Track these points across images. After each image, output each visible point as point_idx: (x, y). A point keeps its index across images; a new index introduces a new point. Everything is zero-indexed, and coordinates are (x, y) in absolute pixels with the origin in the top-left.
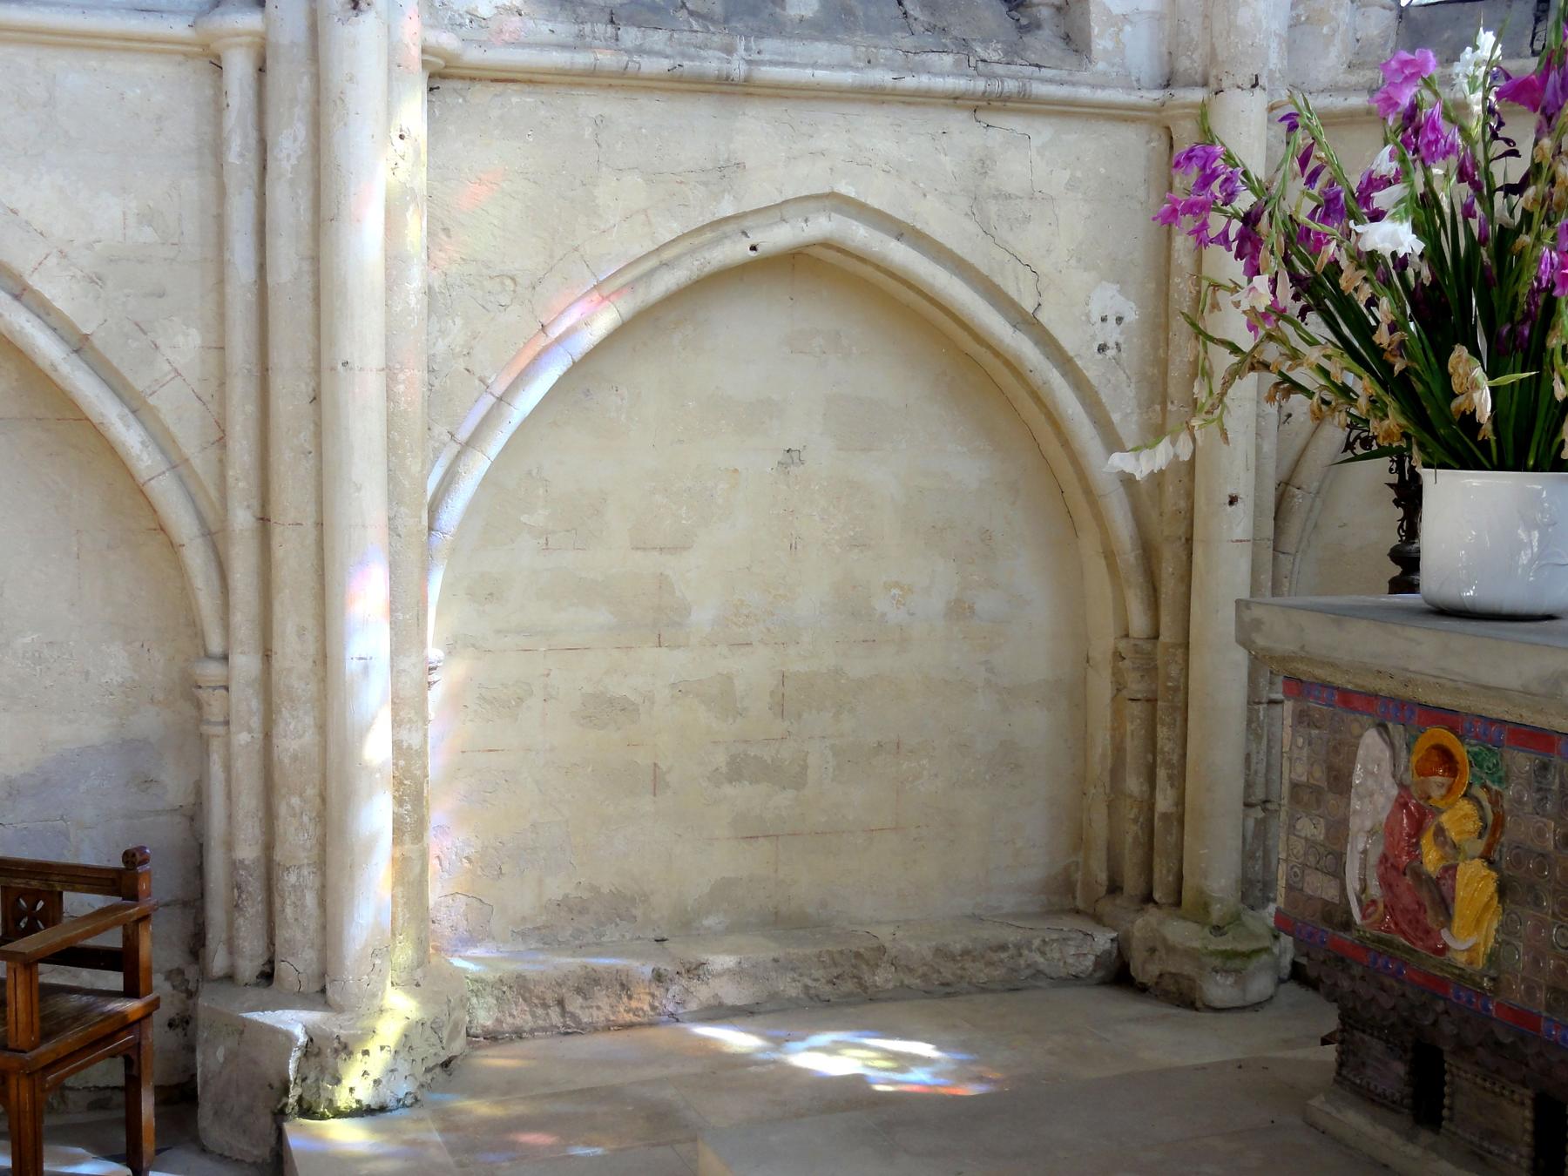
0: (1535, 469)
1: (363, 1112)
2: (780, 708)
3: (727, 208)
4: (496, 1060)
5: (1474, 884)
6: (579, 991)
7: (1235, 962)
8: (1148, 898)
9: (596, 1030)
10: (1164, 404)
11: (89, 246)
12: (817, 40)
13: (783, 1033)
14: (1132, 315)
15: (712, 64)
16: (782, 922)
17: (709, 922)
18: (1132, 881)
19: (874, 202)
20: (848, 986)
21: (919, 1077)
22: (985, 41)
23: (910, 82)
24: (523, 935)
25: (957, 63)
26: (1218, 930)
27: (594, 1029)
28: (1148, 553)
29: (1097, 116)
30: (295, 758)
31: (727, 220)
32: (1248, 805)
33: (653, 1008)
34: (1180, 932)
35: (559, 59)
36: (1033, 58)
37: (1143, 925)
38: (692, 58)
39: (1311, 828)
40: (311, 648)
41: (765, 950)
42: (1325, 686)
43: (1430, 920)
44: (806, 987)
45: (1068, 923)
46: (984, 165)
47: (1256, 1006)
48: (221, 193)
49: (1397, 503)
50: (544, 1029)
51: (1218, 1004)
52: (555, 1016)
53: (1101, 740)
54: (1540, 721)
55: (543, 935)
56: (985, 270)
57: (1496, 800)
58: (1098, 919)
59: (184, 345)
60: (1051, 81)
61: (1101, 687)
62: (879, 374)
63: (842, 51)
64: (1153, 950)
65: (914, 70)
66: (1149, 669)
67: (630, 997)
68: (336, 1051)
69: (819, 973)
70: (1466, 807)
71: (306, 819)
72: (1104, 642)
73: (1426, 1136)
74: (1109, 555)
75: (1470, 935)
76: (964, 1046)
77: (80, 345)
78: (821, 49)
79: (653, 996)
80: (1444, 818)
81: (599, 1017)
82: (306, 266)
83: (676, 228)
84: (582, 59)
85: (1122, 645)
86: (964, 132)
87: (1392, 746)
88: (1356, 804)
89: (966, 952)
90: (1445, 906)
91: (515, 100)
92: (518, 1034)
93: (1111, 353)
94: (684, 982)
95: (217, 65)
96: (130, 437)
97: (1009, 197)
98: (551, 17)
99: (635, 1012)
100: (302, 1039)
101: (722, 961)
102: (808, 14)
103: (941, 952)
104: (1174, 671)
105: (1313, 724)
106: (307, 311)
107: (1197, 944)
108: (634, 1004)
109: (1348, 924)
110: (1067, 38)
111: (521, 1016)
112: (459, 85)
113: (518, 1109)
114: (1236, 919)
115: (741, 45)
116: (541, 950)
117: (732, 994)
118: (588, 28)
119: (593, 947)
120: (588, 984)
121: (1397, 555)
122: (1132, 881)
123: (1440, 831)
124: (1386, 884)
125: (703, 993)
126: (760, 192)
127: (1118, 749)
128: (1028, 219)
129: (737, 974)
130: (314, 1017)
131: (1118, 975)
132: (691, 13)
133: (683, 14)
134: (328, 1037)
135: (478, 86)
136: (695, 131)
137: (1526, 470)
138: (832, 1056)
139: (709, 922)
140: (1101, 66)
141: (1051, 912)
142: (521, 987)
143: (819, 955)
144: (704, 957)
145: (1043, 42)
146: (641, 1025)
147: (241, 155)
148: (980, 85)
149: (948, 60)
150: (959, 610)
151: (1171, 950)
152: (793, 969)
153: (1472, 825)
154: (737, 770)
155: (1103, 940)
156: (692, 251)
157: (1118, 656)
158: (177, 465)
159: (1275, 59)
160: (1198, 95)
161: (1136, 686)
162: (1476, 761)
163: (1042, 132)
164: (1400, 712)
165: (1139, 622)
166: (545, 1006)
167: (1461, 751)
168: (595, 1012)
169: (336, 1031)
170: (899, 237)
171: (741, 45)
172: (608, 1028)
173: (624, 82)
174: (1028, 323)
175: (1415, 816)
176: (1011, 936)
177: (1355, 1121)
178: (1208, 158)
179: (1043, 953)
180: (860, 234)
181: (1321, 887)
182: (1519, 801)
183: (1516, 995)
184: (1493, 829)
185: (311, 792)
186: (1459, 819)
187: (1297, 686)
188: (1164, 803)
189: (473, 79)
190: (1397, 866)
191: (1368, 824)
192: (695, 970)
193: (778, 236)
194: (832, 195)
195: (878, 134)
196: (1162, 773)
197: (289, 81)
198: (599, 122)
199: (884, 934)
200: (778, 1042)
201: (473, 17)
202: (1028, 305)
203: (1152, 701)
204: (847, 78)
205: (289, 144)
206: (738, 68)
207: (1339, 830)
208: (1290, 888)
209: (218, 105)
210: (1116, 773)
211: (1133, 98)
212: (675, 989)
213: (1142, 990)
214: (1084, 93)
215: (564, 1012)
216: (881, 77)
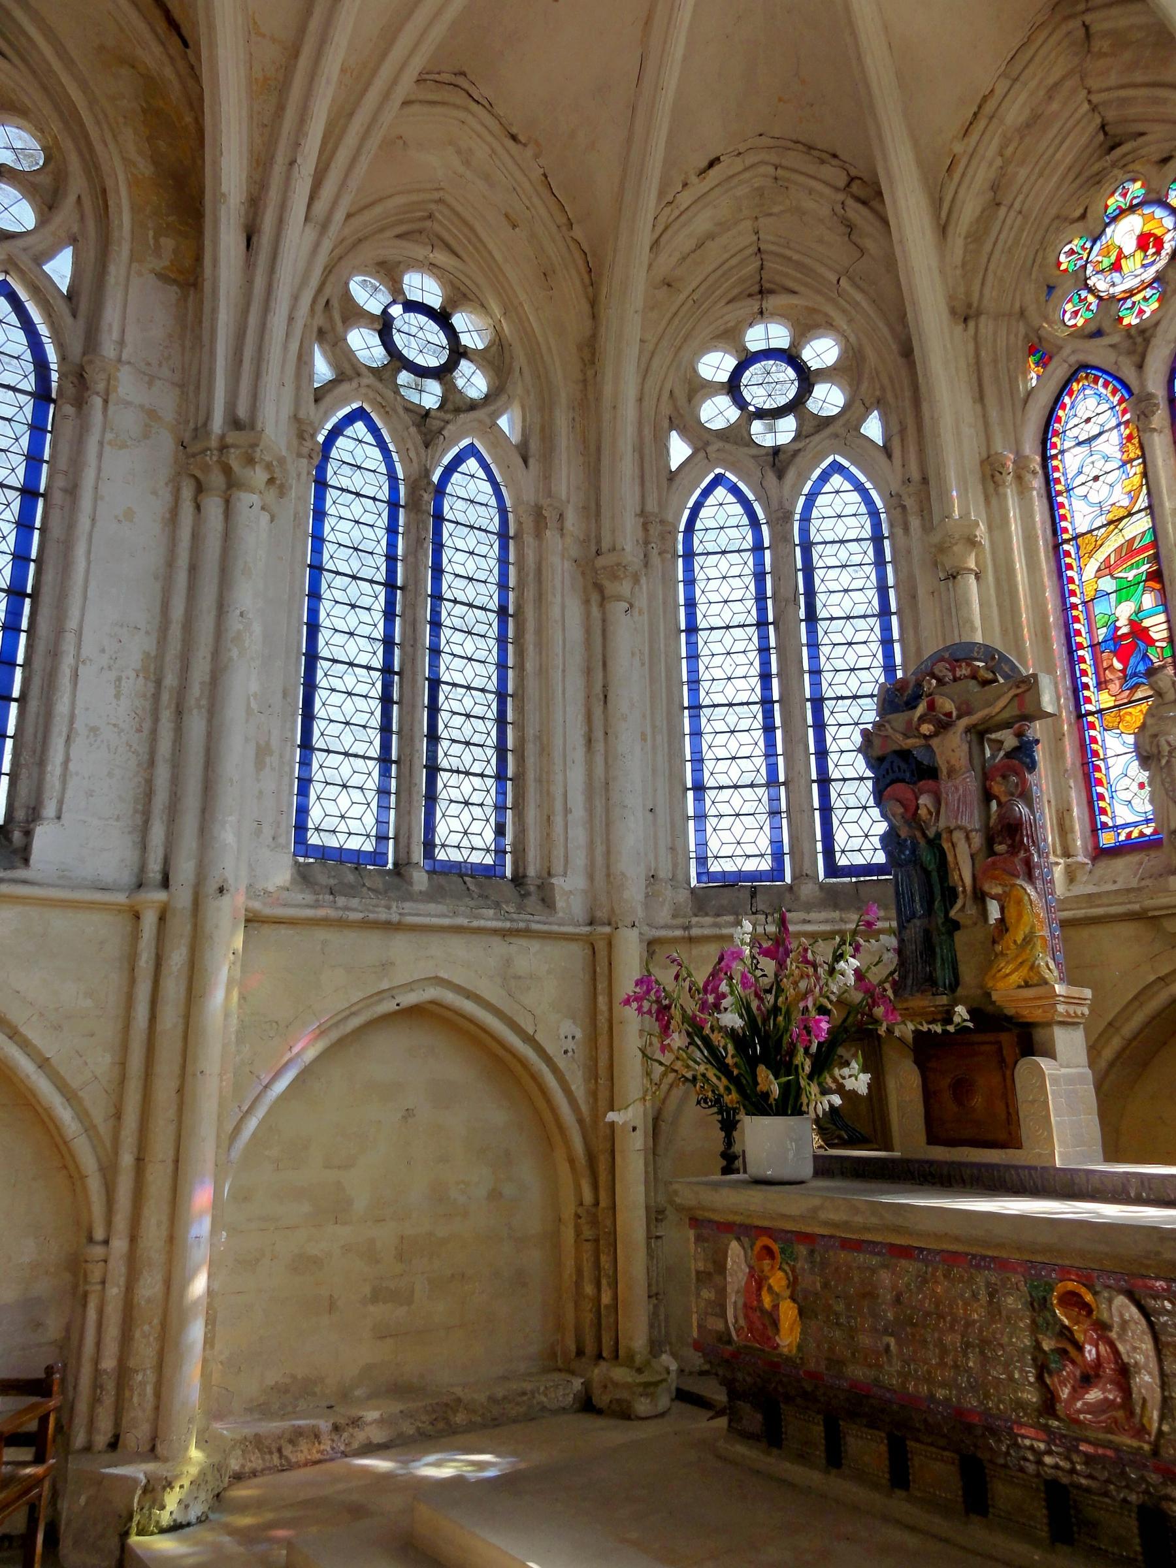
0: (792, 1115)
1: (176, 1527)
2: (400, 1257)
3: (385, 985)
4: (242, 1492)
5: (788, 1312)
6: (291, 1441)
7: (649, 1389)
8: (600, 1356)
9: (299, 1466)
10: (596, 1081)
11: (57, 1009)
12: (429, 902)
13: (410, 1458)
14: (579, 1035)
15: (383, 916)
16: (398, 1389)
17: (357, 1393)
18: (590, 1348)
19: (456, 981)
20: (441, 1425)
21: (491, 1473)
22: (507, 903)
23: (475, 923)
24: (249, 1410)
25: (495, 914)
26: (639, 1371)
27: (298, 1466)
29: (560, 938)
30: (149, 1301)
31: (384, 991)
32: (649, 1297)
33: (333, 1449)
34: (620, 1374)
35: (309, 913)
36: (529, 910)
37: (598, 1372)
38: (373, 912)
39: (707, 1294)
40: (164, 1233)
41: (396, 1407)
42: (710, 1221)
43: (770, 1333)
44: (418, 1428)
45: (556, 1376)
46: (508, 962)
47: (662, 1415)
48: (132, 981)
49: (722, 1129)
50: (270, 1469)
51: (643, 1415)
52: (276, 1460)
53: (569, 1264)
54: (809, 1230)
55: (263, 1410)
56: (509, 1014)
57: (793, 1270)
58: (573, 1373)
59: (102, 1062)
60: (539, 922)
61: (568, 1234)
62: (453, 1067)
63: (441, 908)
64: (605, 1387)
65: (477, 917)
66: (594, 1222)
67: (320, 1443)
68: (164, 1488)
69: (424, 1418)
70: (780, 1274)
71: (151, 1339)
72: (569, 1210)
73: (775, 1451)
74: (571, 1161)
75: (788, 1338)
76: (514, 1453)
77: (43, 1063)
78: (432, 907)
79: (333, 1441)
80: (771, 1281)
81: (301, 1457)
82: (181, 1021)
83: (361, 995)
84: (321, 913)
85: (580, 1211)
86: (499, 947)
87: (744, 1248)
88: (729, 1279)
89: (505, 1398)
90: (775, 1324)
91: (283, 932)
92: (254, 1474)
93: (570, 1054)
94: (351, 1430)
95: (137, 917)
96: (65, 1115)
97: (520, 977)
98: (302, 891)
99: (322, 1452)
100: (144, 1481)
101: (372, 1415)
102: (423, 889)
103: (492, 1399)
104: (609, 1223)
105: (705, 1240)
106: (179, 1044)
107: (630, 1380)
108: (322, 1447)
109: (730, 1341)
110: (543, 900)
111: (256, 1461)
112: (256, 925)
113: (269, 1516)
114: (648, 1363)
115: (394, 905)
116: (260, 1420)
117: (378, 1435)
118: (321, 897)
119: (291, 1417)
120: (295, 1437)
121: (724, 1155)
122: (590, 1348)
123: (770, 1288)
124: (746, 1316)
125: (361, 1436)
126: (401, 978)
127: (579, 1271)
128: (529, 988)
129: (381, 1422)
130: (150, 1467)
131: (587, 1405)
132: (369, 889)
133: (364, 890)
134: (160, 1479)
135: (266, 925)
136: (372, 946)
137: (786, 1115)
138: (437, 1468)
139: (357, 1393)
140: (561, 914)
141: (546, 1370)
142: (257, 1442)
143: (425, 1407)
144: (361, 1413)
145: (532, 901)
146: (326, 1461)
147: (147, 962)
148: (508, 925)
149: (491, 912)
150: (495, 1195)
151: (616, 1385)
152: (411, 1417)
153: (784, 1283)
154: (377, 1296)
155: (577, 1384)
156: (368, 1006)
157: (578, 1216)
158: (89, 1129)
159: (640, 913)
160: (607, 929)
161: (588, 1233)
162: (783, 1251)
163: (535, 946)
164: (745, 1231)
165: (588, 1197)
166: (271, 1453)
167: (775, 1247)
168: (299, 1455)
169: (165, 1474)
170: (468, 998)
171: (394, 905)
172: (306, 1465)
173: (341, 924)
174: (530, 1040)
175: (758, 1281)
176: (528, 1386)
177: (741, 1449)
178: (649, 983)
179: (546, 1395)
180: (450, 997)
181: (715, 1324)
182: (803, 1269)
183: (812, 1365)
184: (793, 1284)
185: (156, 1321)
186: (778, 1280)
187: (695, 1222)
188: (606, 1299)
189: (263, 922)
190: (752, 1307)
191: (736, 1288)
192: (356, 1422)
193: (410, 999)
194: (436, 977)
195: (458, 947)
196: (604, 1282)
197: (180, 927)
198: (325, 943)
199: (458, 1391)
200: (405, 1463)
201: (266, 892)
202: (531, 1032)
203: (597, 1241)
204: (446, 922)
205: (177, 958)
206: (395, 918)
207: (722, 1292)
208: (700, 1327)
209: (136, 935)
210: (578, 1285)
211: (577, 930)
212: (345, 1435)
213: (599, 1412)
214: (555, 928)
215: (281, 1456)
216: (462, 921)
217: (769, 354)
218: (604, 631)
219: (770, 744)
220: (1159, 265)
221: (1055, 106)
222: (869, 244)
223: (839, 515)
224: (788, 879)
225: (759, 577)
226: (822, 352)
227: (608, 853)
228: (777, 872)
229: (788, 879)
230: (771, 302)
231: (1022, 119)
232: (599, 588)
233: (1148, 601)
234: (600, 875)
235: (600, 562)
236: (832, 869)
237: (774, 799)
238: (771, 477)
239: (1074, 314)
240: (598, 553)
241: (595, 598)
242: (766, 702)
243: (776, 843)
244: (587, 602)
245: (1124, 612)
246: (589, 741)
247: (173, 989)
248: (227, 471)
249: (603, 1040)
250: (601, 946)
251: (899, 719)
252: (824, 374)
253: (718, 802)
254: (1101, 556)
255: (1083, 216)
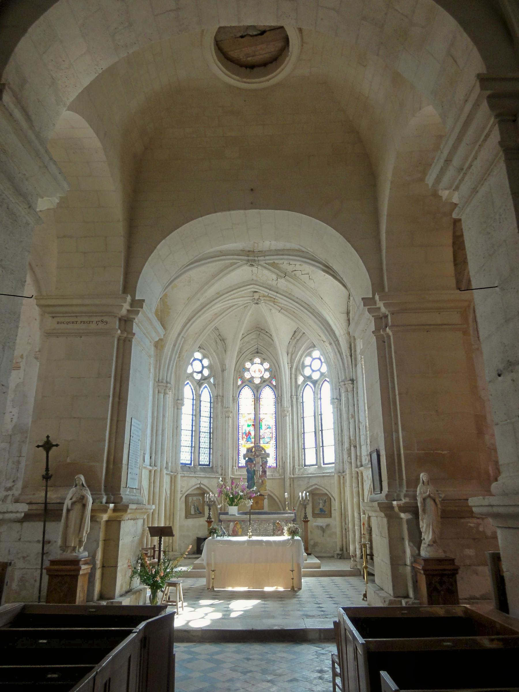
28: (170, 515)
217: (198, 359)
218: (177, 415)
219: (192, 439)
220: (261, 375)
221: (252, 342)
222: (219, 347)
223: (206, 395)
224: (192, 465)
225: (193, 405)
226: (206, 362)
227: (176, 459)
228: (191, 464)
229: (192, 465)
230: (202, 350)
231: (247, 340)
232: (177, 406)
233: (252, 429)
234: (174, 463)
235: (179, 401)
236: (200, 465)
237: (192, 450)
238: (198, 387)
239: (247, 375)
240: (178, 400)
241: (176, 408)
242: (192, 431)
243: (191, 458)
244: (174, 407)
245: (248, 429)
246: (173, 436)
247: (157, 484)
248: (165, 390)
249: (173, 494)
250: (173, 477)
251: (250, 453)
252: (206, 367)
253: (183, 449)
254: (245, 419)
255: (251, 360)
